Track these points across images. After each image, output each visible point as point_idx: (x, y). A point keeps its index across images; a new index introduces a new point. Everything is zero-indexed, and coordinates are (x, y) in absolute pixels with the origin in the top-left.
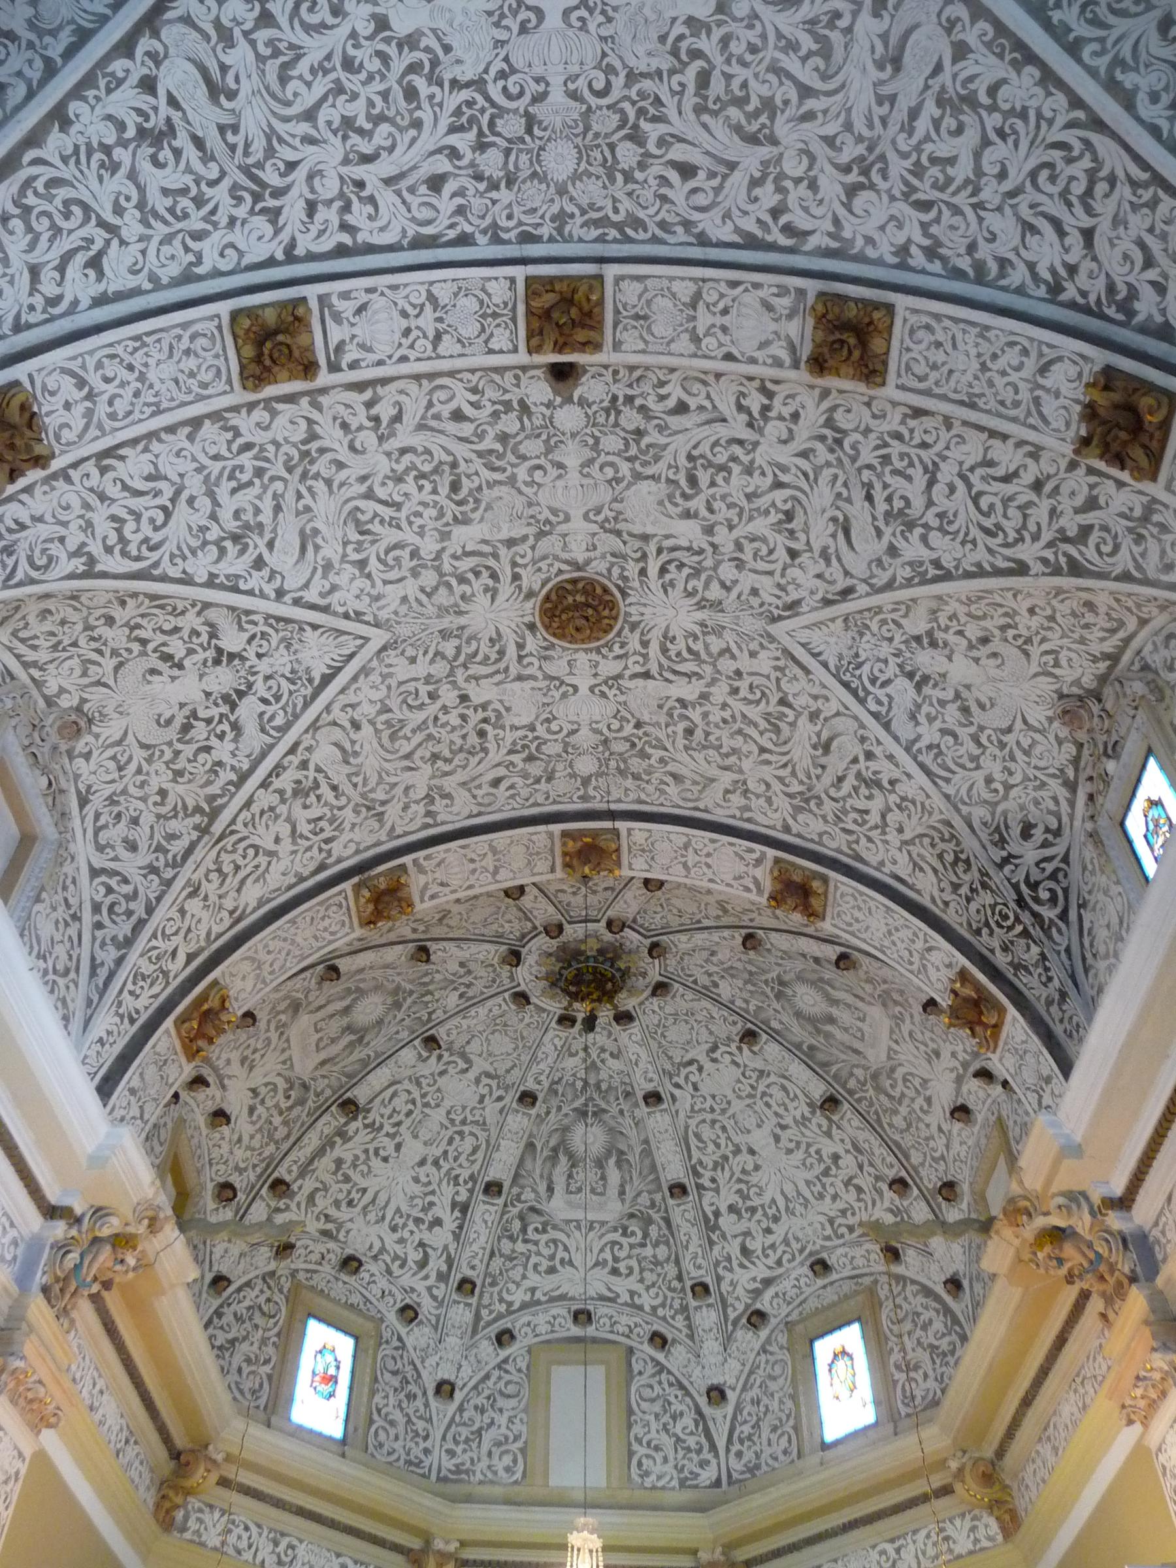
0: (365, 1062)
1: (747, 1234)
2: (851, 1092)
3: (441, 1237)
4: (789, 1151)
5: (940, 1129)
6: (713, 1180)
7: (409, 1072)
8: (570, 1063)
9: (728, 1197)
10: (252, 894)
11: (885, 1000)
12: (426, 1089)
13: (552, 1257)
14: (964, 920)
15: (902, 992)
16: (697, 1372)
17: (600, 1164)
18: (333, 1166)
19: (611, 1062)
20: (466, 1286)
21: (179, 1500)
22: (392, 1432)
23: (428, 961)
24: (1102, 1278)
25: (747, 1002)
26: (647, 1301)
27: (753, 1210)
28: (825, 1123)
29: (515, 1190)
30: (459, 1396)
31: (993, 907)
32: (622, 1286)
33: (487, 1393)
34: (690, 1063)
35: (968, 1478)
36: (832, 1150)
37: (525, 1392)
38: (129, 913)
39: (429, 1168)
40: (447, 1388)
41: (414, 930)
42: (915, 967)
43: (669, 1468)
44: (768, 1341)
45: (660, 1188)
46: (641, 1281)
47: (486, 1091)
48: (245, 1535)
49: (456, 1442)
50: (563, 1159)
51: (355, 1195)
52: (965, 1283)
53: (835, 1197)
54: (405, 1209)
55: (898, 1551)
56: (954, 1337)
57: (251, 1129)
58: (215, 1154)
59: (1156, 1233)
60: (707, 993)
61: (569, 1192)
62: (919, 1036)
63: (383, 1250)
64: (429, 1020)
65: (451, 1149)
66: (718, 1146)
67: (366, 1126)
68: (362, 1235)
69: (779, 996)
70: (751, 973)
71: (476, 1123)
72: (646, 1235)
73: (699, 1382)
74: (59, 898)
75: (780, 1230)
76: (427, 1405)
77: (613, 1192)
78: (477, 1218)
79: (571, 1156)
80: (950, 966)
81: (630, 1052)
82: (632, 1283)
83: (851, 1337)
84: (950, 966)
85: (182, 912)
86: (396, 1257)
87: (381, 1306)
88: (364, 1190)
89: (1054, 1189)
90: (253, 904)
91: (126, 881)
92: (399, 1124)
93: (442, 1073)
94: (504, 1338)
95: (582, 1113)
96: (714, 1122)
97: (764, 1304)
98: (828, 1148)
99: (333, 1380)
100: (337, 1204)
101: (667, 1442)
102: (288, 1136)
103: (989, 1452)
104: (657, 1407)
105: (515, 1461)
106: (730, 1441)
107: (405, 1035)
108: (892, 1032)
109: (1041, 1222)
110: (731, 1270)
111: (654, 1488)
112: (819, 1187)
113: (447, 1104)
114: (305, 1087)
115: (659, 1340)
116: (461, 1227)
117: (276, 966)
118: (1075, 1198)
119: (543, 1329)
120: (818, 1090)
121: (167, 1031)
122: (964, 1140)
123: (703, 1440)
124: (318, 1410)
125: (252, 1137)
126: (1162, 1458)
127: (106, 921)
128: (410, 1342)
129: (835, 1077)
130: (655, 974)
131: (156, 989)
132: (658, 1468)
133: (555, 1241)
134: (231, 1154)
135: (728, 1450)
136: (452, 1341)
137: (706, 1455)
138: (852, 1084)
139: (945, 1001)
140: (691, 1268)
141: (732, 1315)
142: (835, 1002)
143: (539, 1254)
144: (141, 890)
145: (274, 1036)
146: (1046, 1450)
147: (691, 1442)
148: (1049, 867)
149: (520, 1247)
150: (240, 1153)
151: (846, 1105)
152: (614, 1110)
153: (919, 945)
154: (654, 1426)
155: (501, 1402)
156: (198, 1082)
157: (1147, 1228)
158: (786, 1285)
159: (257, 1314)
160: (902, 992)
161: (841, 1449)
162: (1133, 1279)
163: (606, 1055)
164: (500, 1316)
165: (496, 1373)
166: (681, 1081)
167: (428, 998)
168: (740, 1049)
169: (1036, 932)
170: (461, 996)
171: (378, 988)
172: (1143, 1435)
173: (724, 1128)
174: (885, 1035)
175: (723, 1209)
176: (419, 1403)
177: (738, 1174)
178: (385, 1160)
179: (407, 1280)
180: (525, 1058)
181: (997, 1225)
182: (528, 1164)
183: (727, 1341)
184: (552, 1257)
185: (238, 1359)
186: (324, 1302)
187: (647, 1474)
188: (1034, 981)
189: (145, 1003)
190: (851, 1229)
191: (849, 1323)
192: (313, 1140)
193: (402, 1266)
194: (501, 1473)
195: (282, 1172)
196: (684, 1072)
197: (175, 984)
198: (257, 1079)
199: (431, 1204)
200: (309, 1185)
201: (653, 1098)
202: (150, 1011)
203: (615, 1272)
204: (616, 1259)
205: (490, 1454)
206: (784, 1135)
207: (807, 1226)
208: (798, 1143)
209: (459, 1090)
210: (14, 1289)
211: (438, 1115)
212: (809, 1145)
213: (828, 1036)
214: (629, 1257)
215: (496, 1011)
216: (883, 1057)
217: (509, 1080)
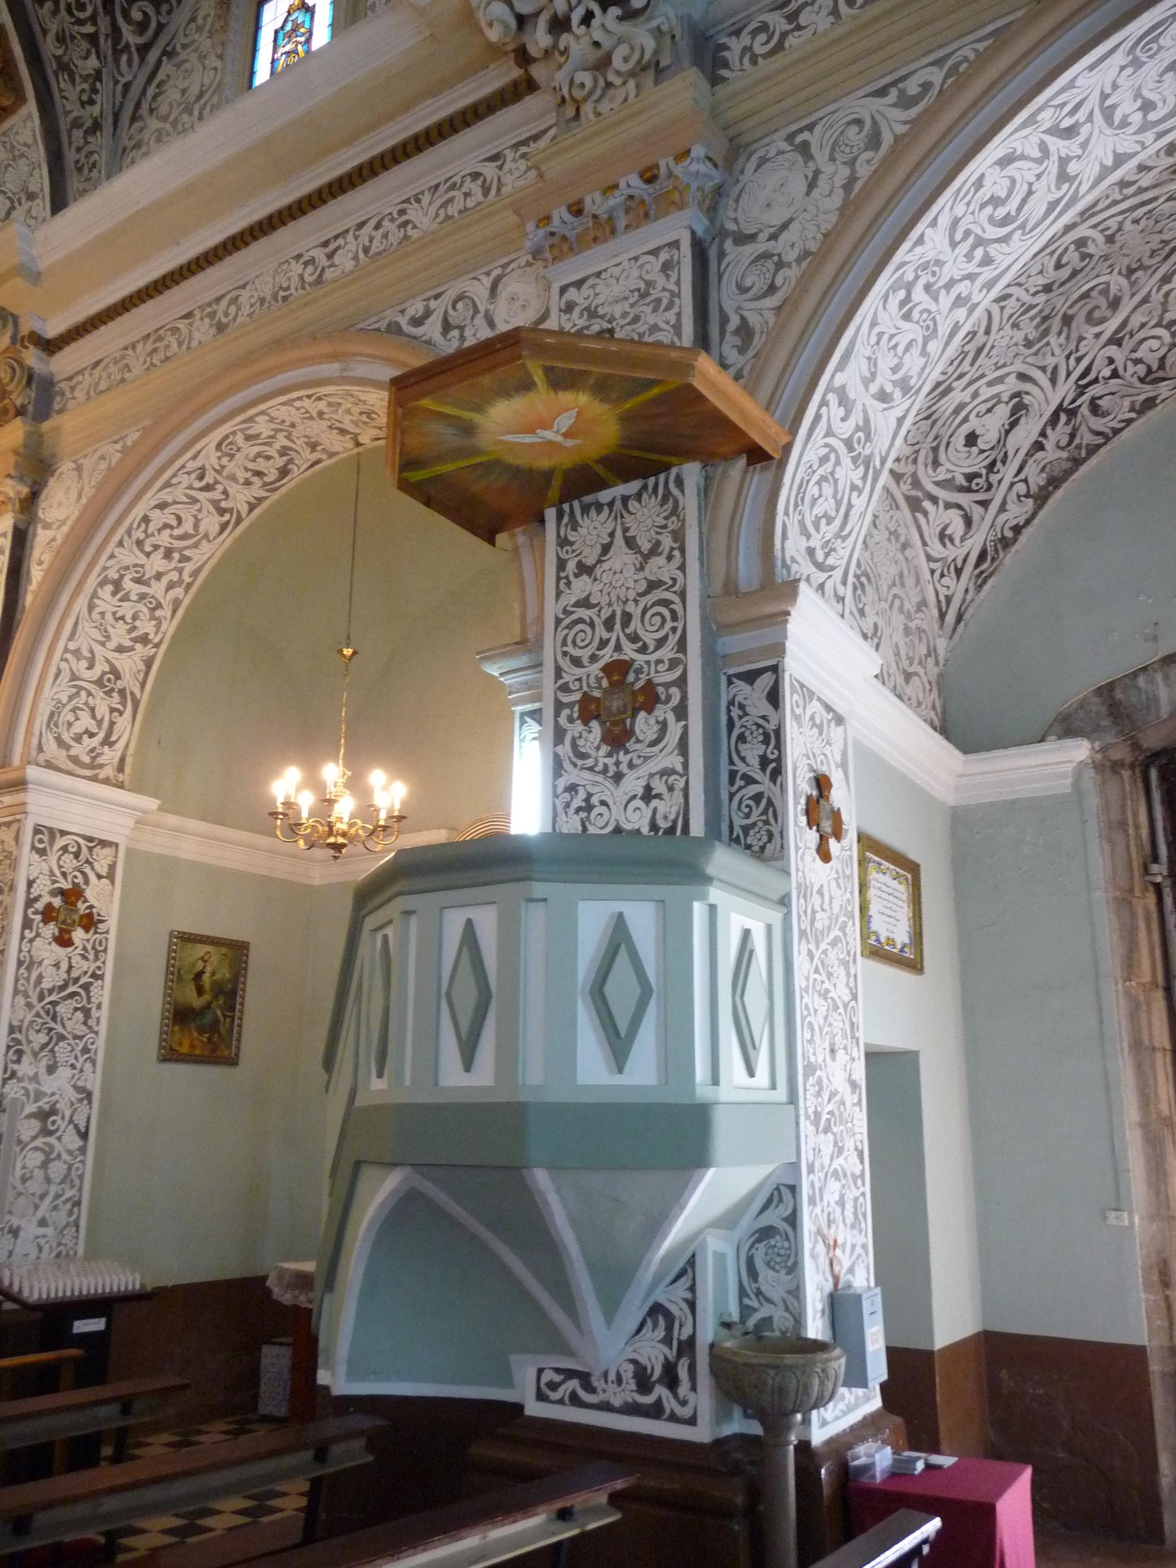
59: (64, 386)
157: (57, 378)
162: (20, 412)
169: (106, 45)
188: (72, 93)
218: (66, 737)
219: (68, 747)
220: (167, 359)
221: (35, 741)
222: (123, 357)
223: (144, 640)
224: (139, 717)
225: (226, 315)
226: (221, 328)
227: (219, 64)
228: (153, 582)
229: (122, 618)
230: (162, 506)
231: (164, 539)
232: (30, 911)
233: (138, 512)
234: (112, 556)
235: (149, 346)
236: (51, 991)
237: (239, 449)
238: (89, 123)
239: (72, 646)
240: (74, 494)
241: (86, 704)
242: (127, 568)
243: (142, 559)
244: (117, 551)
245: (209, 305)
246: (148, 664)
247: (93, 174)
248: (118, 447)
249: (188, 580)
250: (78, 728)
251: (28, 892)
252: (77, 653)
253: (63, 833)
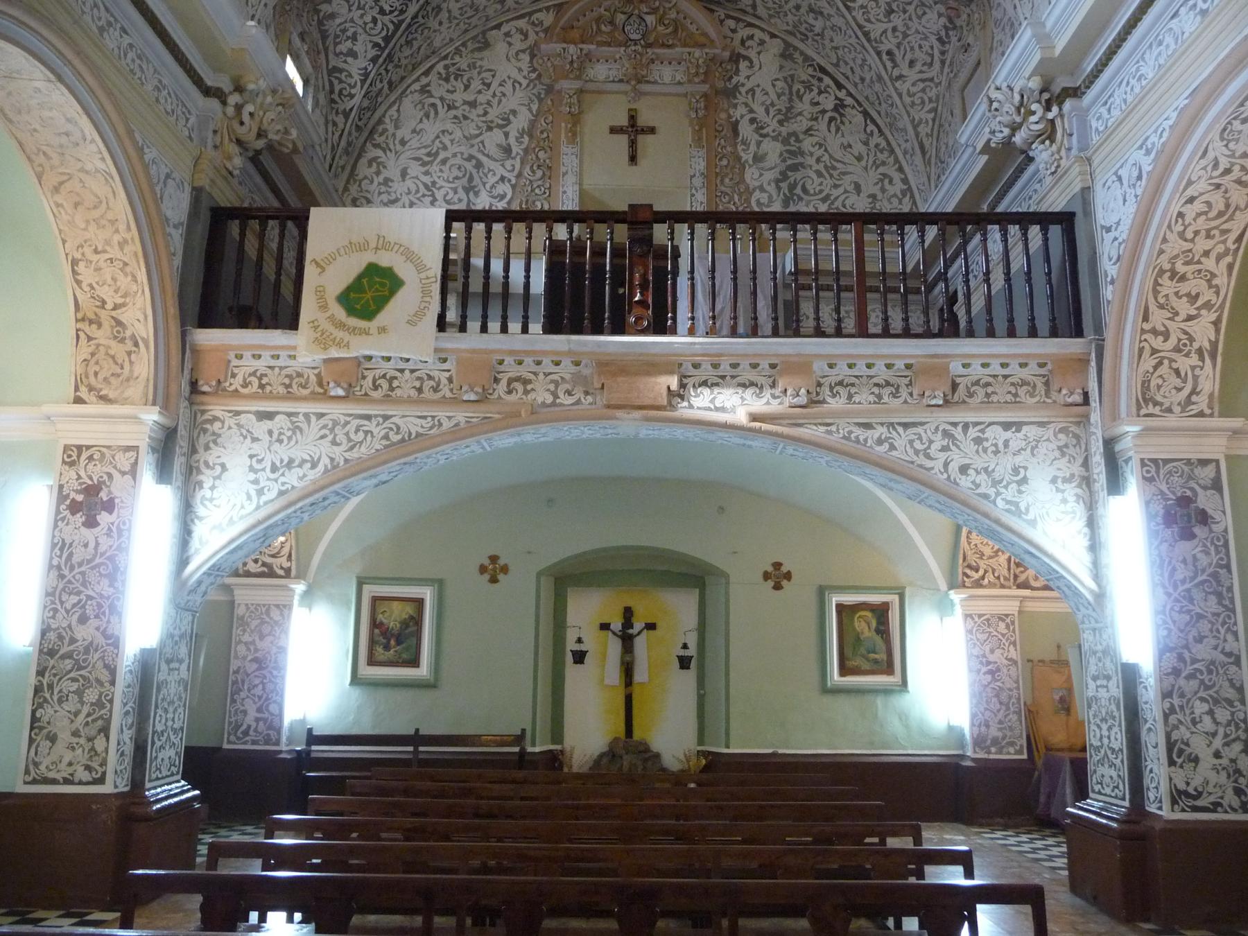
223: (1208, 305)
228: (1203, 259)
231: (1201, 223)
242: (1176, 256)
246: (1216, 323)
249: (1233, 247)
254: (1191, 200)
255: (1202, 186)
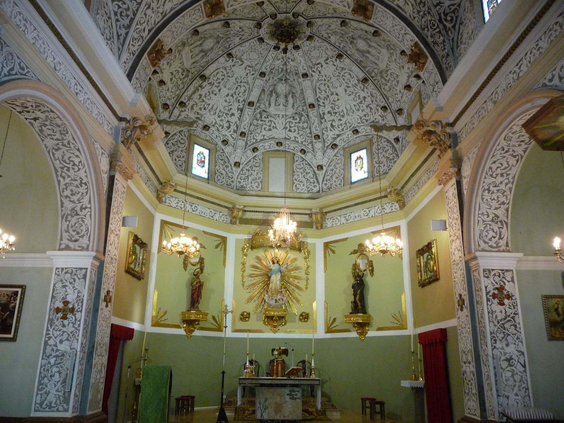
0: (207, 62)
1: (333, 120)
2: (372, 77)
3: (234, 119)
4: (350, 95)
5: (400, 92)
6: (323, 103)
7: (222, 65)
8: (277, 62)
9: (328, 108)
10: (168, 6)
11: (388, 47)
12: (228, 71)
13: (270, 126)
14: (420, 24)
15: (394, 46)
16: (314, 161)
17: (286, 97)
18: (198, 97)
19: (291, 63)
20: (243, 134)
21: (163, 195)
22: (222, 176)
23: (229, 27)
24: (441, 145)
25: (340, 44)
26: (300, 140)
27: (336, 113)
28: (362, 86)
29: (258, 105)
30: (241, 166)
31: (430, 21)
32: (292, 135)
33: (250, 165)
34: (319, 64)
35: (392, 194)
36: (364, 95)
37: (262, 165)
38: (127, 16)
39: (230, 97)
40: (238, 164)
41: (224, 16)
42: (400, 39)
43: (305, 187)
44: (337, 153)
45: (306, 105)
46: (298, 134)
47: (248, 72)
48: (183, 204)
49: (241, 179)
50: (274, 95)
51: (206, 106)
52: (401, 140)
53: (363, 111)
54: (222, 110)
55: (369, 211)
56: (394, 155)
57: (172, 86)
58: (161, 94)
60: (327, 40)
61: (276, 105)
62: (398, 61)
63: (216, 123)
64: (229, 47)
65: (237, 91)
66: (326, 92)
67: (209, 84)
68: (209, 119)
69: (351, 43)
70: (342, 34)
71: (245, 82)
72: (300, 120)
73: (315, 163)
74: (103, 11)
75: (344, 120)
76: (232, 169)
77: (290, 105)
78: (246, 113)
79: (277, 94)
80: (412, 40)
81: (298, 60)
82: (295, 134)
83: (363, 153)
84: (412, 40)
85: (145, 14)
86: (220, 125)
87: (216, 140)
88: (209, 104)
89: (432, 120)
90: (169, 10)
91: (124, 3)
92: (219, 83)
93: (233, 66)
94: (255, 150)
95: (281, 80)
96: (325, 84)
97: (337, 142)
98: (362, 94)
99: (204, 162)
100: (200, 109)
101: (304, 180)
102: (183, 87)
103: (399, 188)
104: (302, 171)
105: (259, 185)
106: (323, 180)
107: (221, 53)
108: (389, 58)
109: (426, 128)
110: (327, 131)
111: (300, 193)
112: (358, 107)
113: (235, 76)
114: (188, 71)
115: (303, 151)
116: (240, 116)
117: (179, 32)
118: (438, 122)
119: (267, 147)
120: (361, 75)
121: (145, 58)
122: (408, 96)
123: (315, 180)
124: (200, 171)
125: (172, 88)
126: (447, 194)
127: (120, 19)
128: (226, 151)
129: (368, 72)
130: (308, 32)
131: (140, 43)
132: (301, 187)
133: (271, 121)
134: (167, 94)
135: (322, 183)
136: (239, 150)
137: (316, 184)
138: (373, 74)
139: (408, 52)
140: (314, 130)
141: (326, 145)
142: (370, 46)
143: (266, 125)
144: (130, 6)
145: (177, 54)
146: (416, 188)
147: (312, 180)
148: (453, 8)
149: (260, 122)
150: (169, 94)
151: (370, 81)
152: (292, 79)
153: (403, 32)
154: (301, 176)
155: (254, 168)
156: (155, 72)
157: (457, 132)
158: (344, 137)
159: (179, 143)
160: (394, 46)
161: (356, 184)
162: (450, 147)
163: (290, 60)
164: (253, 143)
165: (253, 160)
166: (315, 70)
167: (229, 40)
168: (336, 60)
169: (443, 32)
170: (240, 39)
171: (211, 37)
172: (443, 188)
173: (328, 86)
174: (387, 59)
175: (326, 112)
176: (230, 168)
177: (332, 102)
178: (215, 94)
179: (224, 132)
180: (262, 61)
181: (413, 128)
182: (262, 96)
183: (324, 152)
184: (270, 126)
185: (174, 157)
186: (199, 139)
187: (298, 189)
189: (137, 48)
190: (367, 121)
191: (363, 149)
192: (192, 89)
193: (222, 128)
194: (255, 188)
195: (182, 99)
196: (316, 67)
197: (145, 41)
198: (172, 69)
199: (231, 109)
200: (191, 103)
201: (305, 75)
202: (139, 51)
203: (290, 131)
204: (290, 127)
205: (251, 183)
206: (348, 90)
207: (353, 119)
208: (353, 93)
209: (239, 71)
210: (114, 142)
211: (232, 80)
212: (356, 93)
213: (367, 57)
214: (295, 126)
215: (252, 44)
216: (385, 66)
217: (256, 68)
218: (486, 240)
219: (488, 243)
220: (483, 117)
221: (477, 244)
222: (472, 121)
223: (503, 203)
224: (509, 228)
225: (495, 98)
226: (495, 102)
227: (475, 20)
228: (500, 185)
229: (494, 199)
230: (494, 162)
231: (499, 171)
232: (488, 296)
233: (487, 167)
234: (484, 182)
235: (478, 115)
236: (501, 320)
237: (512, 137)
238: (446, 55)
239: (480, 212)
240: (469, 167)
241: (490, 228)
243: (494, 180)
244: (485, 180)
245: (490, 97)
246: (507, 210)
247: (451, 69)
248: (477, 149)
249: (512, 181)
250: (489, 236)
251: (486, 290)
252: (483, 214)
253: (493, 270)
254: (494, 162)
255: (498, 157)
